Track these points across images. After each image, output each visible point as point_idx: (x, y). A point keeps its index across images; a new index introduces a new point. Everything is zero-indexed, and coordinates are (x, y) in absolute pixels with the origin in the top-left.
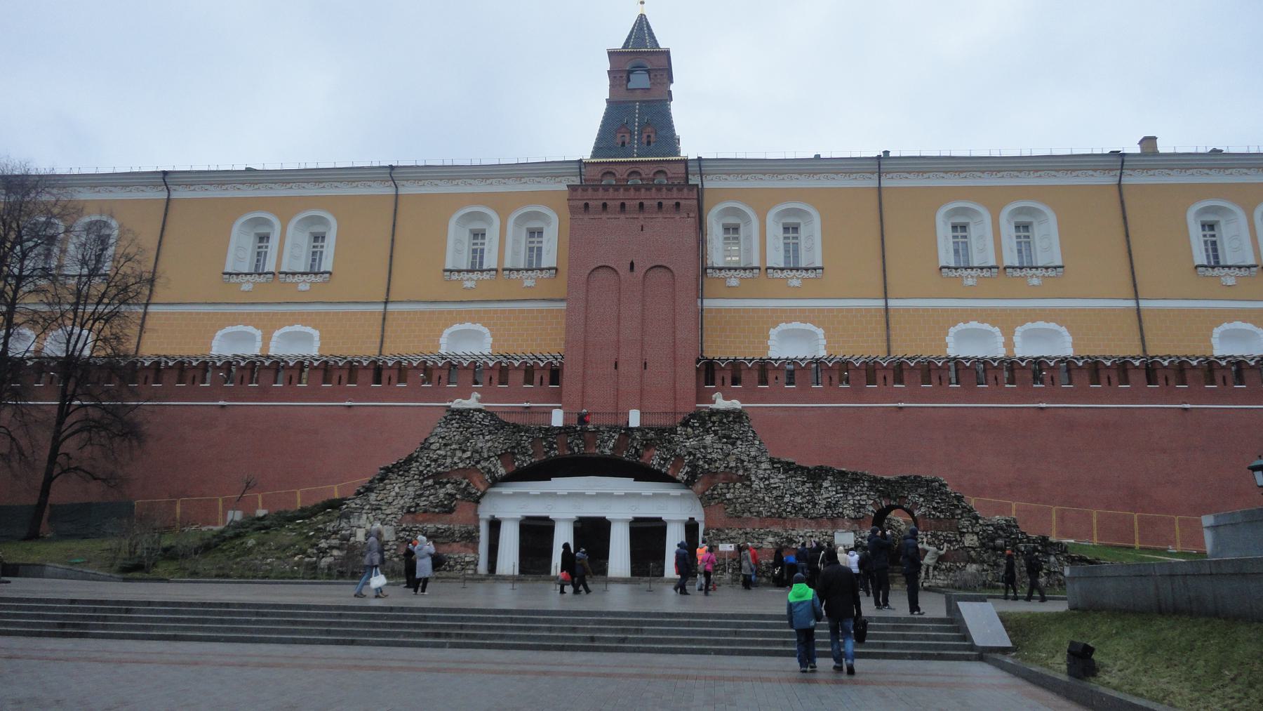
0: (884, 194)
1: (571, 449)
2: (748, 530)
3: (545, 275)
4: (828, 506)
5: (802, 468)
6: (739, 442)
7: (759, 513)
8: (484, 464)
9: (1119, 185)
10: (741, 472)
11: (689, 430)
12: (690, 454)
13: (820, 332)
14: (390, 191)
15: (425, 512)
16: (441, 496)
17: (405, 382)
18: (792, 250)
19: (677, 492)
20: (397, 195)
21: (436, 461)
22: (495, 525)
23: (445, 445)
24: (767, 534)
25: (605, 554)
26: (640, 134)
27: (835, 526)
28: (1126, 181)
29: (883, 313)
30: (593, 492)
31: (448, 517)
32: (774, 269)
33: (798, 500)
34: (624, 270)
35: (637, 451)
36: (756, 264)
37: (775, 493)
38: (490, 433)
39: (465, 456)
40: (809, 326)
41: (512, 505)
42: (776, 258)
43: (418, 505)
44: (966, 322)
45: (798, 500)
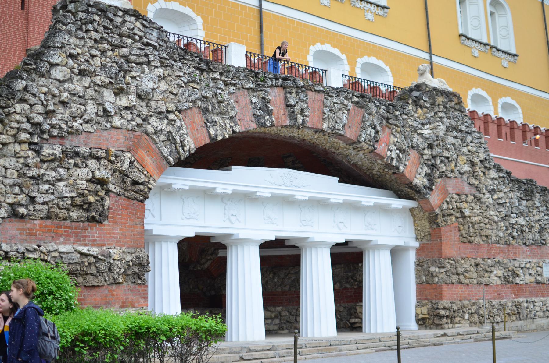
1: (292, 116)
2: (479, 260)
5: (518, 182)
6: (469, 138)
8: (156, 123)
10: (473, 181)
11: (420, 111)
12: (431, 147)
15: (48, 217)
16: (83, 184)
19: (398, 203)
21: (64, 103)
23: (82, 73)
29: (257, 14)
30: (304, 196)
31: (94, 231)
33: (522, 221)
35: (377, 132)
37: (503, 211)
39: (124, 101)
40: (187, 10)
43: (32, 200)
44: (322, 43)
45: (522, 221)
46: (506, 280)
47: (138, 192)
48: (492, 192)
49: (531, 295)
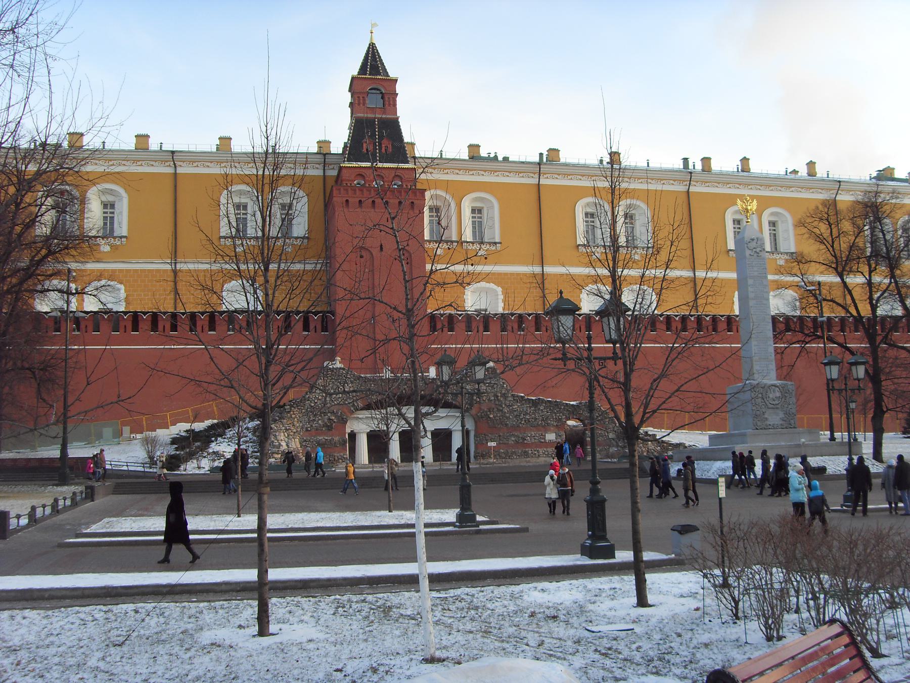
0: (539, 189)
3: (298, 242)
4: (543, 420)
7: (506, 425)
9: (688, 192)
13: (499, 290)
14: (171, 170)
17: (214, 330)
18: (478, 227)
20: (175, 174)
22: (353, 436)
24: (511, 436)
25: (418, 448)
26: (380, 145)
27: (546, 431)
28: (692, 189)
32: (468, 242)
33: (528, 417)
34: (376, 252)
36: (454, 238)
38: (352, 382)
41: (362, 425)
42: (468, 236)
46: (517, 442)
47: (344, 422)
48: (508, 406)
49: (536, 447)
